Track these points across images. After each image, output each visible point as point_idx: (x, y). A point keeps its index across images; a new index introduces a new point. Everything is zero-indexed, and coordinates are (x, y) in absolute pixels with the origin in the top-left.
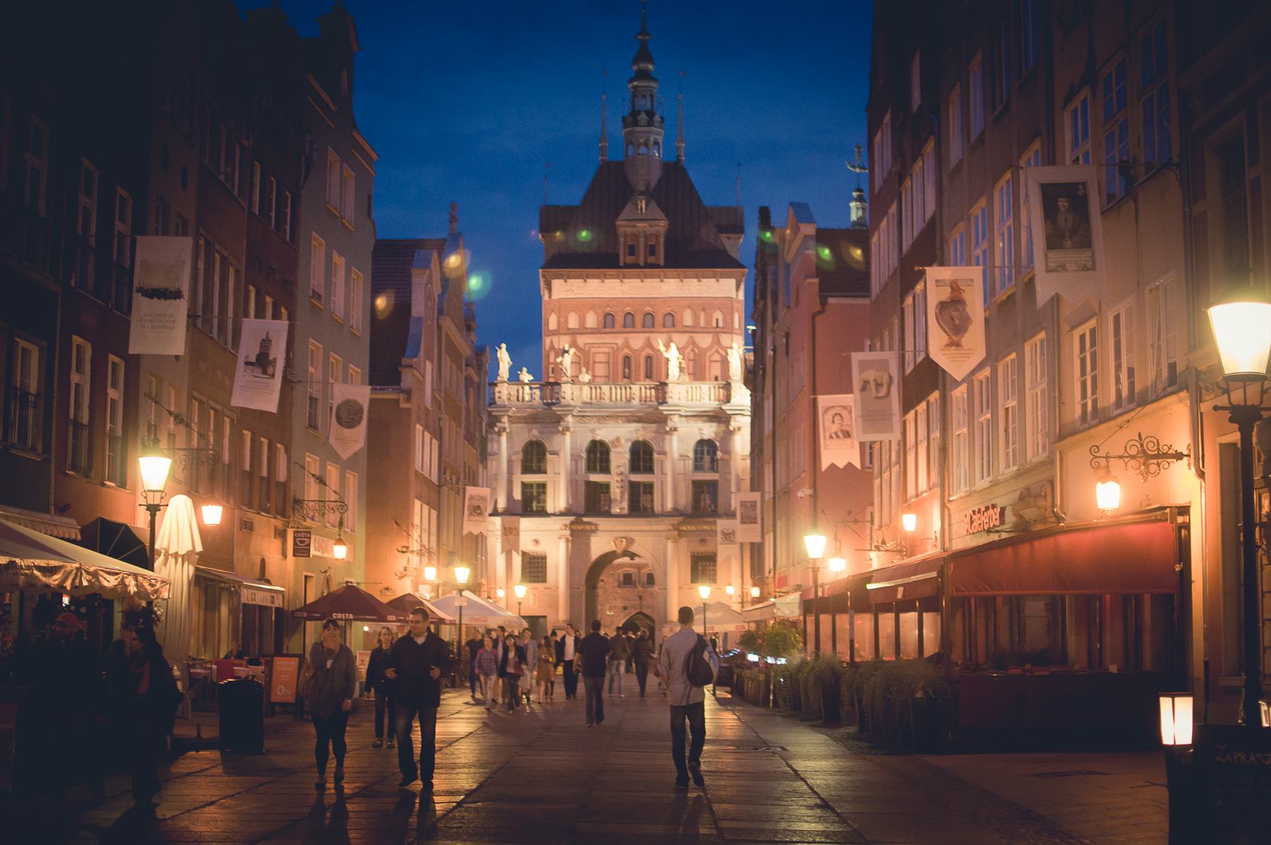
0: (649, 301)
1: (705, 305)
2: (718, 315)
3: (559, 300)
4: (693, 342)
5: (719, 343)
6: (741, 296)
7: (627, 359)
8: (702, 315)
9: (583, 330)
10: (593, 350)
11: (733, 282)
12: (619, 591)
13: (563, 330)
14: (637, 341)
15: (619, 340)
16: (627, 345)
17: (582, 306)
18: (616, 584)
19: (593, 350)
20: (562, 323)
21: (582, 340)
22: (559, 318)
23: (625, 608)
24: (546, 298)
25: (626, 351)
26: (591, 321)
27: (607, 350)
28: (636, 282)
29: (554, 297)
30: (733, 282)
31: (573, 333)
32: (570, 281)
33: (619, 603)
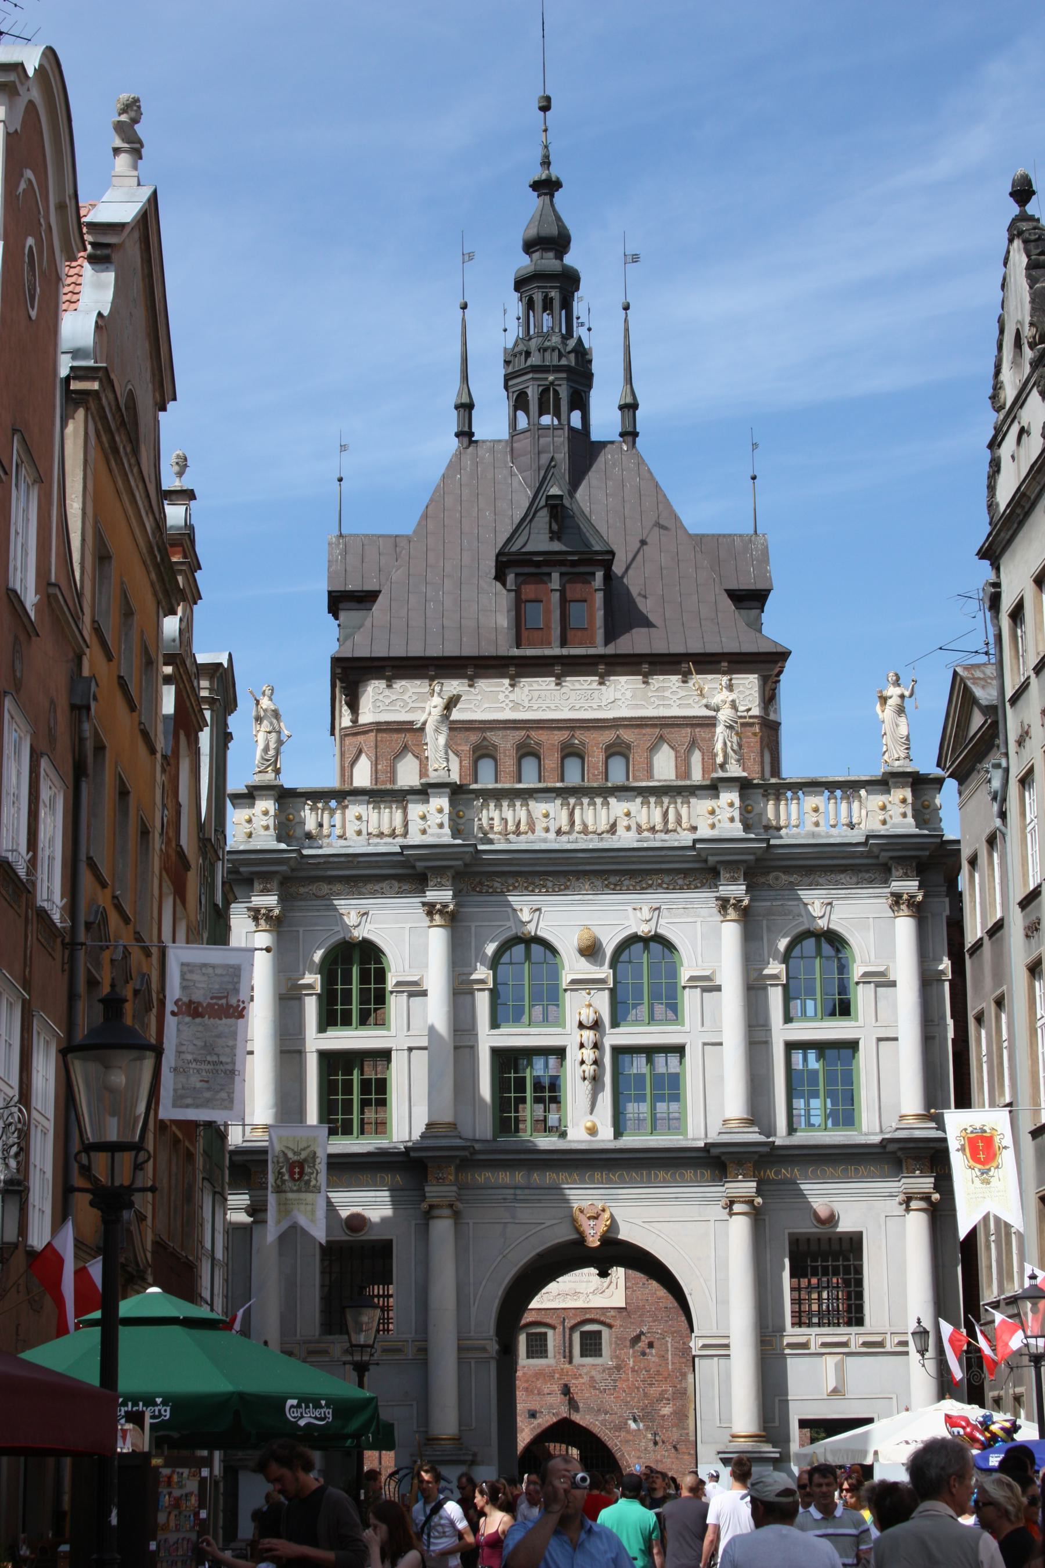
22: (375, 764)
29: (363, 719)
32: (399, 685)
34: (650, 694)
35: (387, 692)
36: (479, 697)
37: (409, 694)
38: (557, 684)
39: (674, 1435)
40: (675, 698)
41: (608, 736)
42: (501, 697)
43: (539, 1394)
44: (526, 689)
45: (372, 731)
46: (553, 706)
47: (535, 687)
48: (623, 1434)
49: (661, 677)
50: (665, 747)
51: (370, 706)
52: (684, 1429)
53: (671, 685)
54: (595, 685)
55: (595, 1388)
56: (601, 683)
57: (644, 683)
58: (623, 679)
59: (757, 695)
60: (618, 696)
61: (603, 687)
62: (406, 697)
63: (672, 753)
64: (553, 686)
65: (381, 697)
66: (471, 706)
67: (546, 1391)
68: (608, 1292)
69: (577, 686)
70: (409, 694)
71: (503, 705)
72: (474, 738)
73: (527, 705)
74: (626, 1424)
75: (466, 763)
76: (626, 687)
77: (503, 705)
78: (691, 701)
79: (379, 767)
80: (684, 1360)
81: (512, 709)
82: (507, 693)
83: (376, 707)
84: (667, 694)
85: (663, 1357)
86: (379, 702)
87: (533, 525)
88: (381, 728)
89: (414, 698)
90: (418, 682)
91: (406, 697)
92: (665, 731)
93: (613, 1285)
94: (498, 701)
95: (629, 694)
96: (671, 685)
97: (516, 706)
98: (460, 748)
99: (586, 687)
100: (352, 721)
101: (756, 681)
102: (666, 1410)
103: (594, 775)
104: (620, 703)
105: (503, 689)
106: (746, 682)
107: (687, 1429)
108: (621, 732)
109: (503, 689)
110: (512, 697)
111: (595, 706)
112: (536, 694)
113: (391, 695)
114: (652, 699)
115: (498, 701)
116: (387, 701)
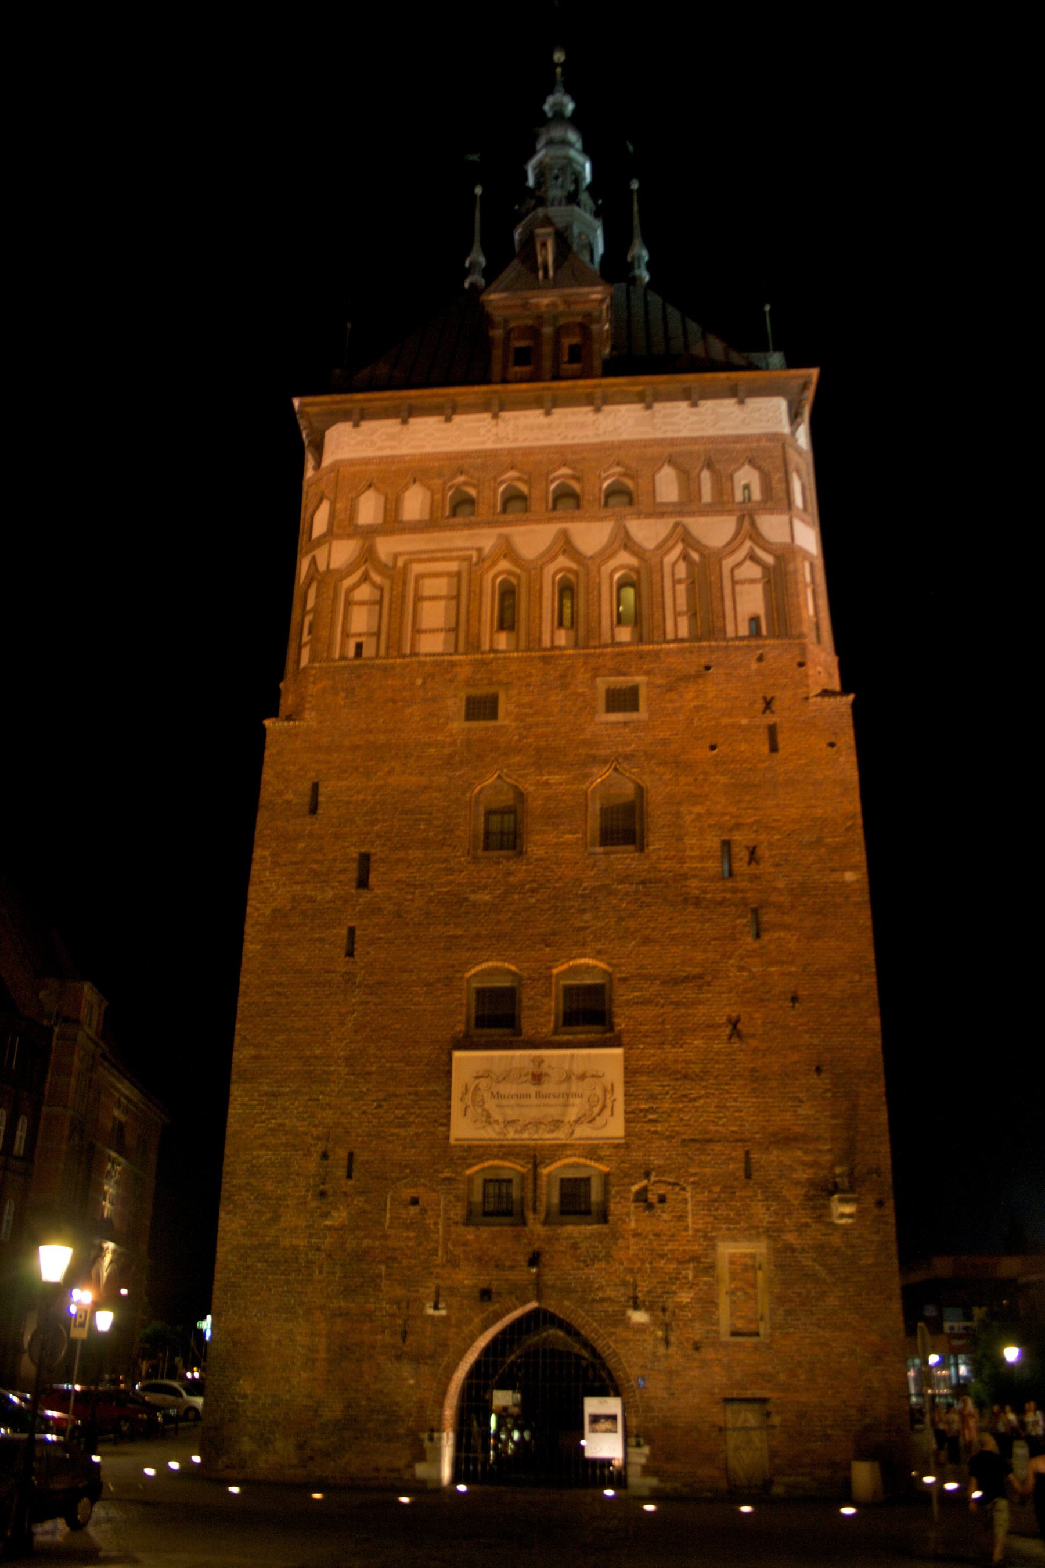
0: (563, 455)
1: (717, 456)
2: (747, 477)
3: (336, 466)
4: (688, 539)
5: (756, 536)
6: (803, 437)
7: (508, 594)
9: (392, 522)
10: (417, 568)
11: (780, 405)
12: (470, 1234)
13: (344, 526)
14: (533, 539)
15: (487, 539)
16: (508, 551)
17: (391, 477)
18: (458, 1212)
19: (417, 568)
20: (344, 526)
23: (486, 1294)
24: (309, 473)
25: (504, 565)
27: (453, 566)
28: (534, 417)
29: (327, 461)
30: (780, 405)
31: (370, 533)
32: (366, 425)
33: (467, 1278)
39: (697, 1331)
42: (482, 431)
43: (497, 1266)
48: (619, 1330)
52: (713, 1324)
55: (578, 1261)
61: (600, 416)
67: (508, 1263)
68: (600, 1121)
73: (511, 437)
74: (624, 1313)
79: (338, 506)
80: (711, 1219)
81: (495, 442)
84: (676, 419)
85: (681, 1218)
93: (607, 1112)
97: (498, 439)
102: (685, 1297)
107: (717, 1323)
109: (485, 423)
110: (494, 430)
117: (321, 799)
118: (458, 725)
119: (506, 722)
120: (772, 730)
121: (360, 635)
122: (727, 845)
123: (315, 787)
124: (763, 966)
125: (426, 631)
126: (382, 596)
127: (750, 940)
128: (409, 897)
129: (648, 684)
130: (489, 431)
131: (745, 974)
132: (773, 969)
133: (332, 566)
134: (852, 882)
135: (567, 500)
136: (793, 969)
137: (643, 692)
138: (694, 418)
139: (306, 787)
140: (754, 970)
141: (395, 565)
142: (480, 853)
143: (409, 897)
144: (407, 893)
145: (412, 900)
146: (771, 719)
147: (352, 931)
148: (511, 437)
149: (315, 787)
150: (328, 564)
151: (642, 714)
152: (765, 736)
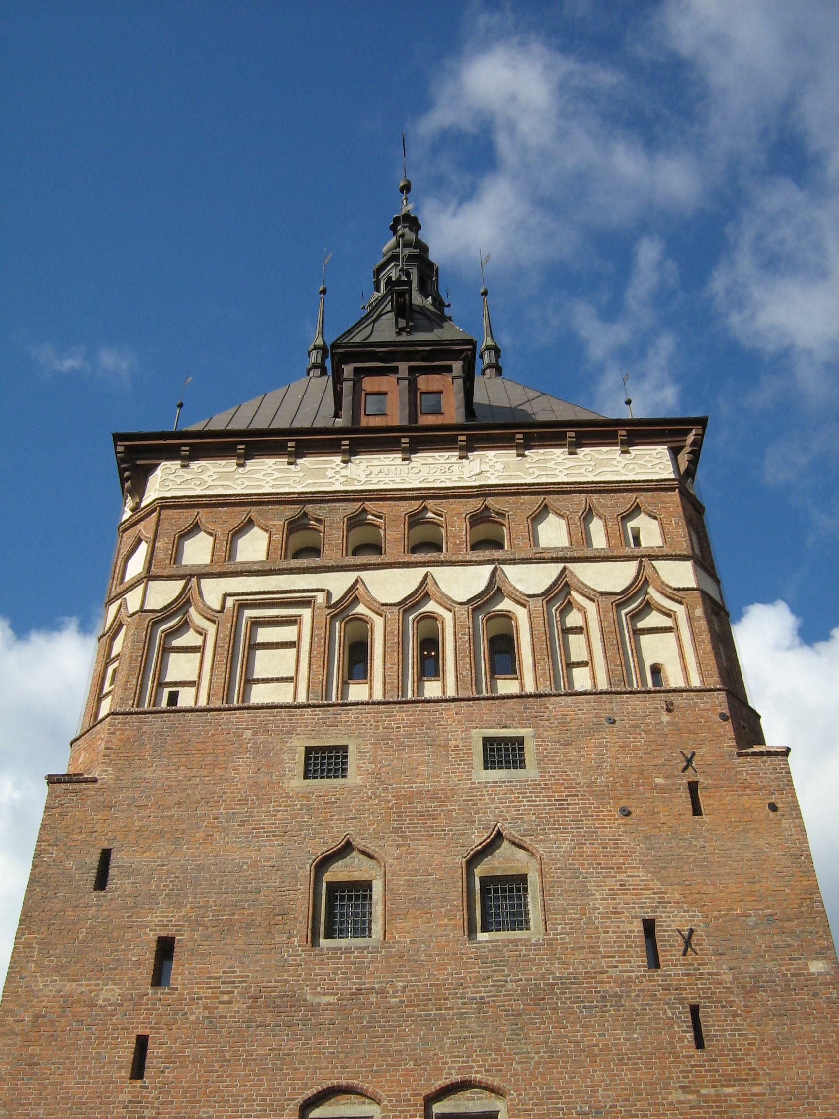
8: (597, 527)
10: (249, 613)
21: (213, 591)
26: (254, 547)
32: (195, 465)
34: (527, 466)
35: (181, 472)
36: (301, 474)
37: (209, 473)
38: (404, 460)
40: (561, 468)
41: (474, 505)
42: (330, 473)
44: (363, 466)
45: (153, 511)
46: (398, 480)
47: (375, 462)
49: (541, 451)
50: (552, 518)
51: (157, 486)
53: (554, 457)
54: (454, 460)
56: (461, 458)
57: (518, 455)
58: (491, 454)
59: (670, 463)
60: (485, 467)
62: (204, 476)
63: (563, 522)
64: (399, 461)
65: (172, 477)
66: (291, 482)
69: (431, 461)
70: (209, 473)
71: (333, 480)
72: (291, 511)
75: (277, 537)
76: (495, 460)
77: (333, 480)
78: (582, 471)
79: (157, 544)
82: (338, 469)
83: (160, 486)
86: (167, 480)
87: (376, 324)
88: (164, 505)
89: (215, 476)
90: (223, 462)
91: (204, 476)
92: (550, 499)
94: (325, 477)
95: (499, 467)
96: (554, 457)
97: (348, 480)
98: (271, 523)
99: (442, 460)
100: (133, 510)
101: (667, 452)
103: (455, 544)
104: (489, 474)
105: (333, 466)
106: (654, 452)
108: (490, 501)
109: (333, 466)
110: (343, 472)
111: (455, 478)
112: (376, 470)
113: (185, 474)
114: (531, 471)
115: (325, 477)
116: (179, 481)
117: (112, 872)
118: (296, 783)
119: (359, 780)
120: (693, 787)
121: (176, 684)
122: (649, 927)
123: (106, 855)
124: (714, 1087)
125: (258, 681)
126: (205, 641)
127: (693, 1051)
128: (226, 998)
129: (536, 736)
130: (337, 472)
131: (691, 1097)
132: (729, 1090)
133: (147, 607)
134: (820, 974)
135: (426, 545)
136: (756, 1090)
137: (530, 747)
138: (569, 464)
139: (94, 860)
140: (703, 1091)
141: (223, 607)
142: (323, 942)
143: (226, 998)
144: (223, 993)
145: (230, 1002)
146: (690, 775)
147: (142, 1043)
148: (364, 479)
149: (106, 855)
150: (143, 604)
151: (531, 772)
152: (685, 795)
